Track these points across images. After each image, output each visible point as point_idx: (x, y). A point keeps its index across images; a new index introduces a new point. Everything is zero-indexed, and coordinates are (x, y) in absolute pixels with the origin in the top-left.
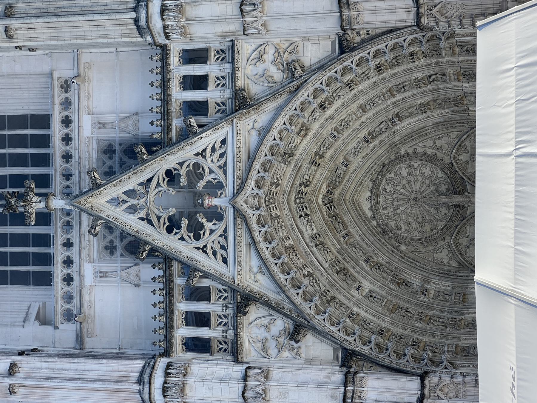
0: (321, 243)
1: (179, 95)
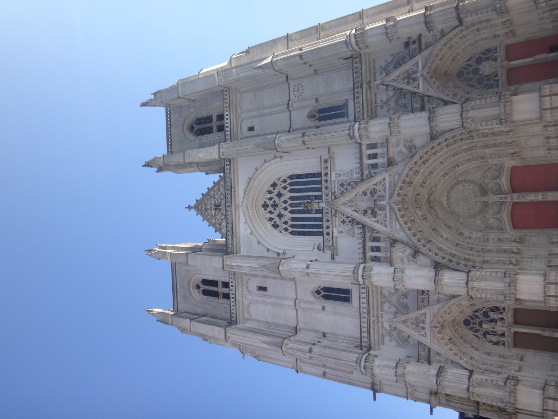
0: (426, 219)
1: (367, 162)
